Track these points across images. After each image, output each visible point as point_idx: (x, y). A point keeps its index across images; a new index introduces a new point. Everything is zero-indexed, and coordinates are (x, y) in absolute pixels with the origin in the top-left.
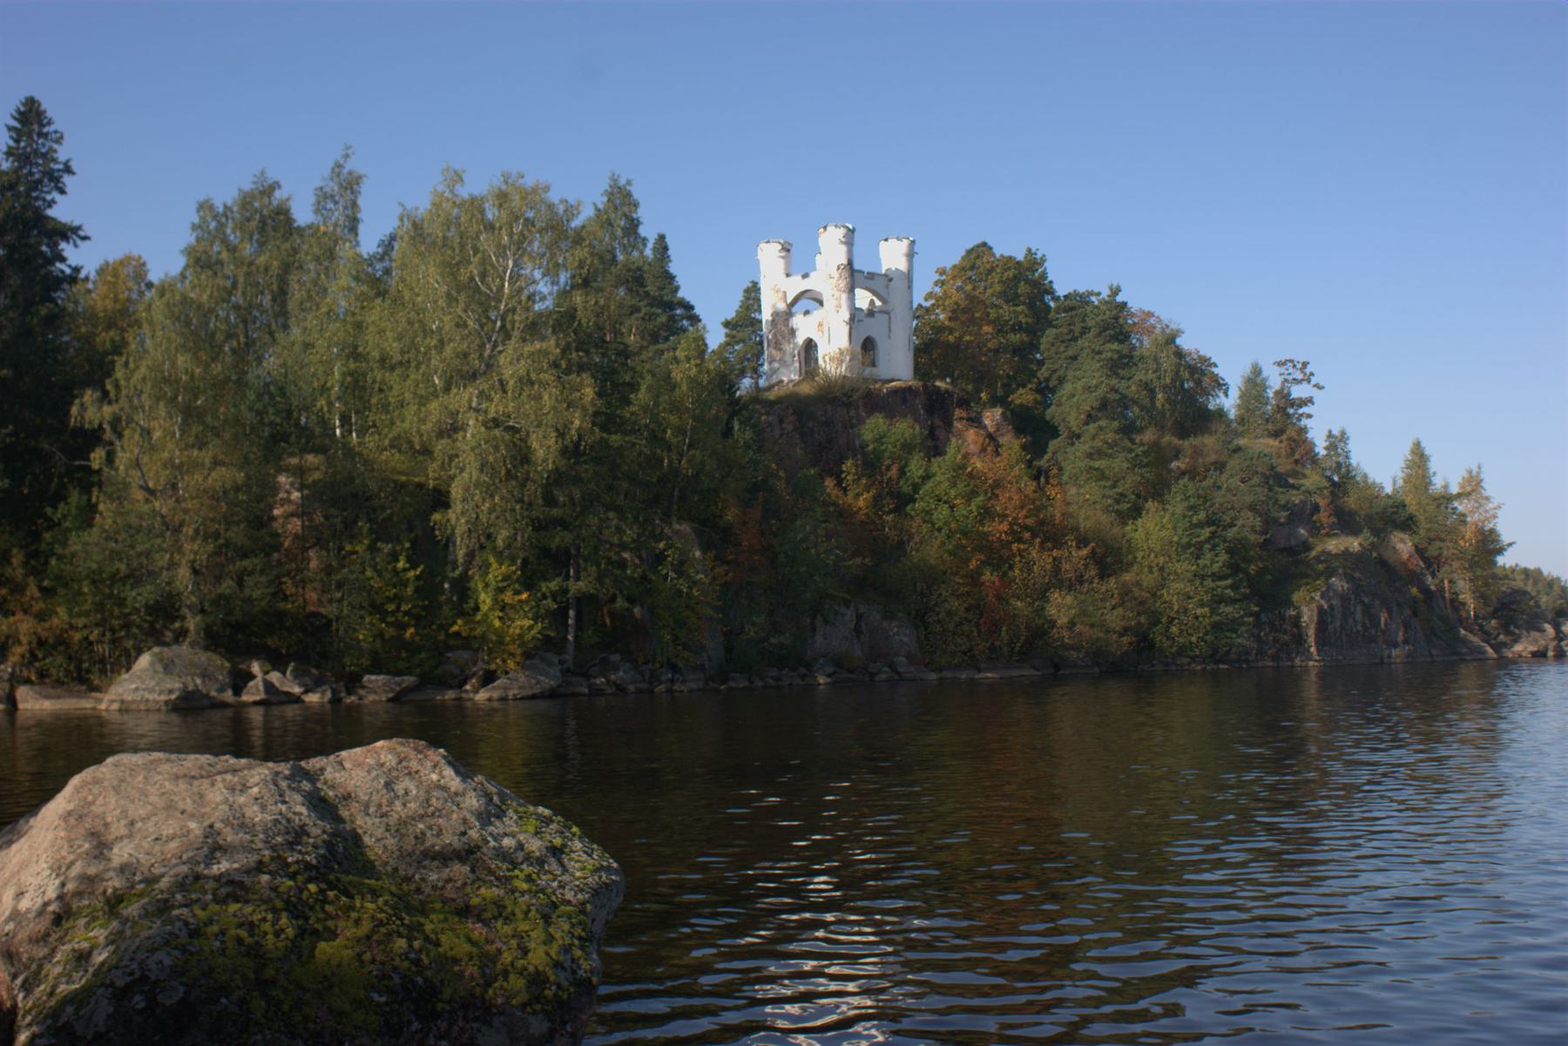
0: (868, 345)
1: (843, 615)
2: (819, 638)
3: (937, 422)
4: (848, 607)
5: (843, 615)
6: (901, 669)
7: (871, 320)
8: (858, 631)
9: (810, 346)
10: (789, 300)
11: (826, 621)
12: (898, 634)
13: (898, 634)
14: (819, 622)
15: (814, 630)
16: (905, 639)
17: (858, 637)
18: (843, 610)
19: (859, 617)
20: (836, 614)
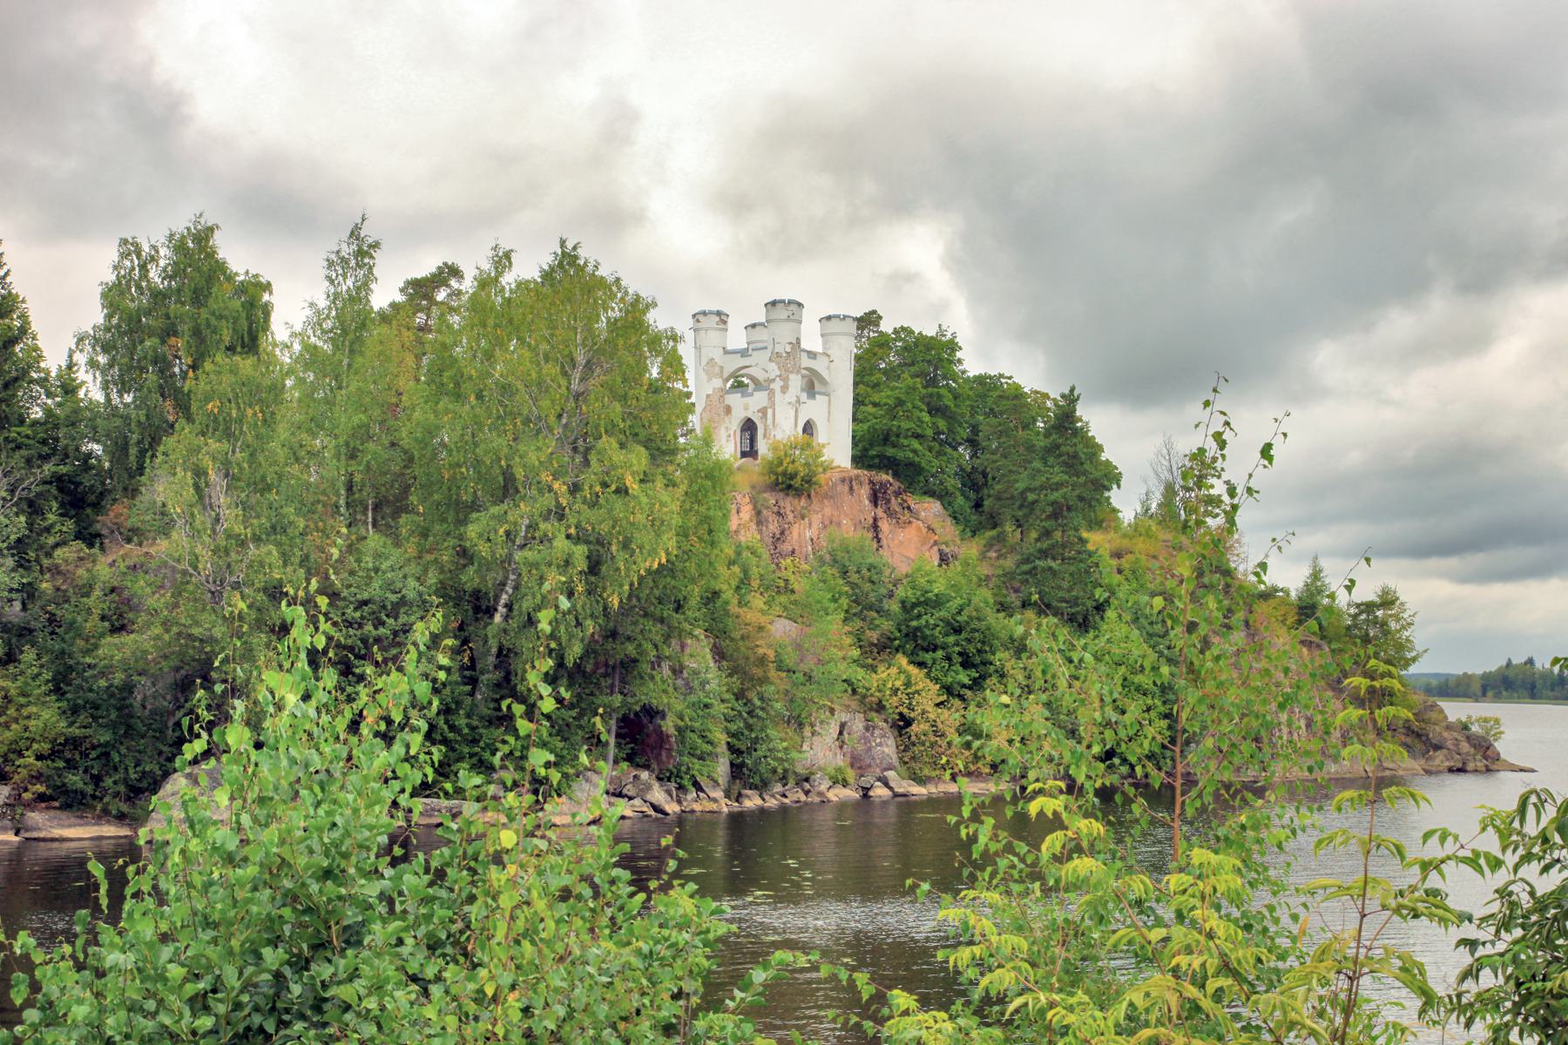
0: (808, 428)
3: (880, 512)
9: (749, 427)
10: (725, 376)
13: (880, 744)
16: (886, 750)
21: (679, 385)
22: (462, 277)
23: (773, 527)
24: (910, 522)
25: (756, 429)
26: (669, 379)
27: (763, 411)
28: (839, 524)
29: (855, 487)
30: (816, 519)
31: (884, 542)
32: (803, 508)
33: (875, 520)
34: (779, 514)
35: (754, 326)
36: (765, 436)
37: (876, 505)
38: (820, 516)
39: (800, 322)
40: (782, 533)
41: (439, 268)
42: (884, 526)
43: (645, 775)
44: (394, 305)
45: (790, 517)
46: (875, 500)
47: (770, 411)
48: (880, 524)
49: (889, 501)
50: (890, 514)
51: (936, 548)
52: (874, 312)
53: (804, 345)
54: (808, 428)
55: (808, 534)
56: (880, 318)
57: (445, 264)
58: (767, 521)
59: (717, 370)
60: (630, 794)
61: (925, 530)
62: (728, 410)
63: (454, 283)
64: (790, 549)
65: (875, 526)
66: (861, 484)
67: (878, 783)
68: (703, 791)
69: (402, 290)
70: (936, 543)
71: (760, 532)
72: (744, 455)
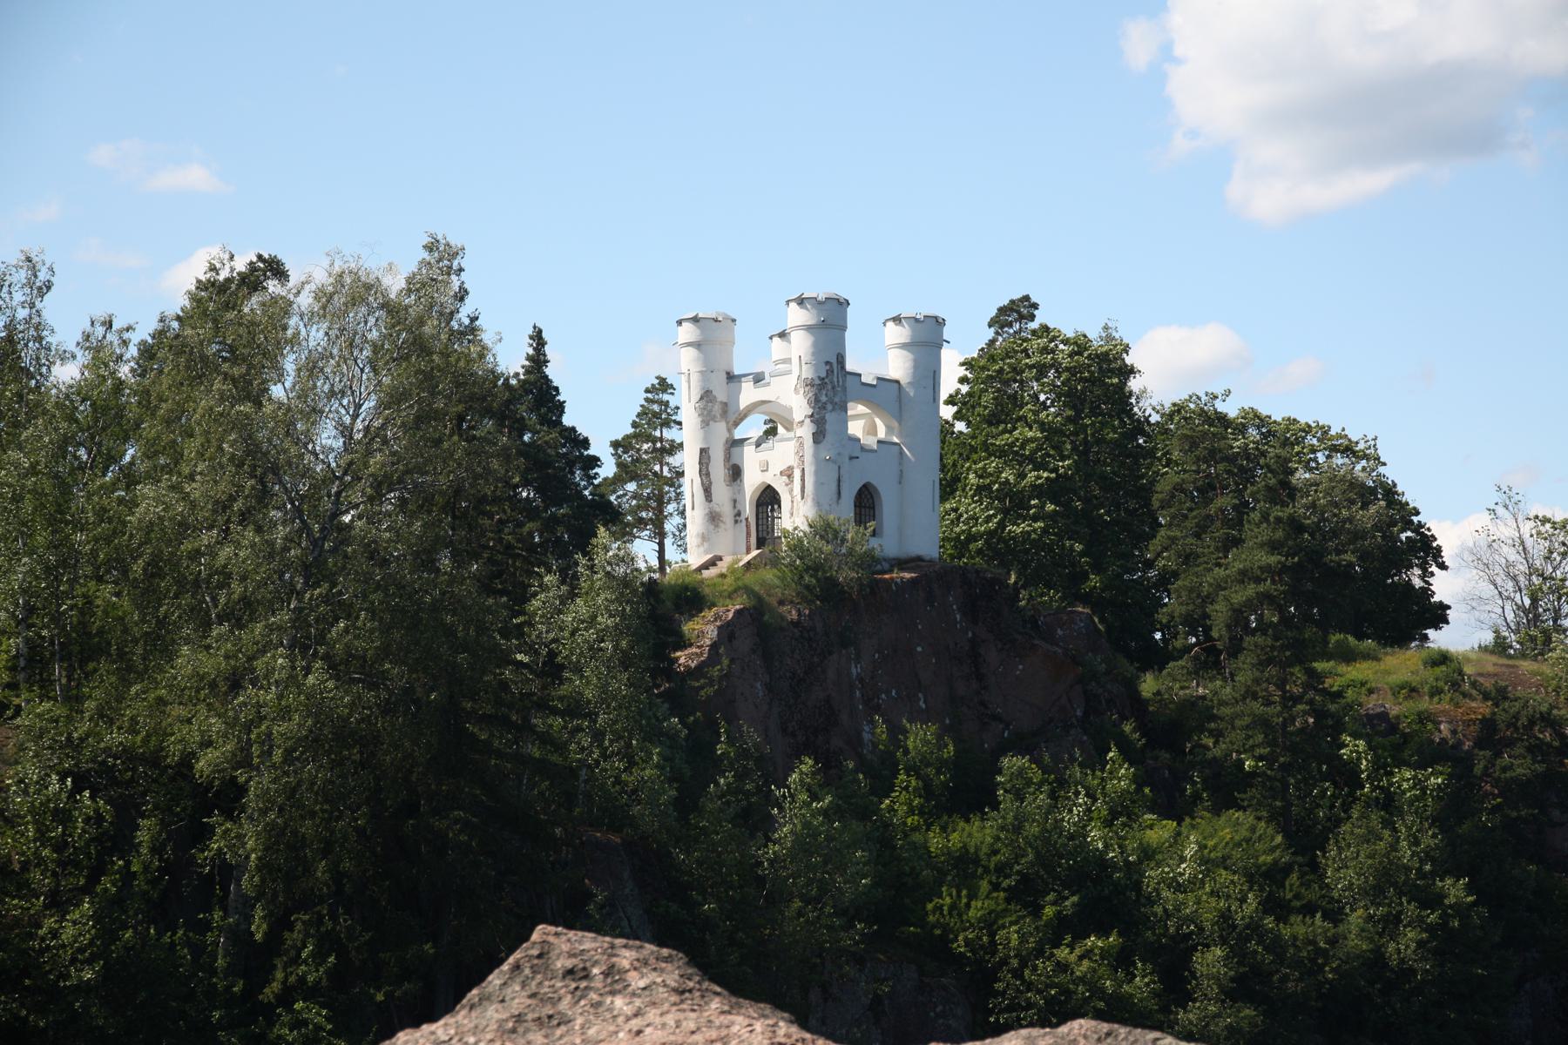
0: (866, 502)
9: (768, 499)
10: (732, 418)
21: (669, 434)
27: (788, 473)
39: (843, 328)
41: (251, 263)
47: (797, 474)
52: (1026, 298)
53: (849, 367)
54: (866, 502)
56: (1035, 306)
57: (260, 257)
59: (717, 409)
62: (736, 473)
63: (273, 286)
72: (761, 543)
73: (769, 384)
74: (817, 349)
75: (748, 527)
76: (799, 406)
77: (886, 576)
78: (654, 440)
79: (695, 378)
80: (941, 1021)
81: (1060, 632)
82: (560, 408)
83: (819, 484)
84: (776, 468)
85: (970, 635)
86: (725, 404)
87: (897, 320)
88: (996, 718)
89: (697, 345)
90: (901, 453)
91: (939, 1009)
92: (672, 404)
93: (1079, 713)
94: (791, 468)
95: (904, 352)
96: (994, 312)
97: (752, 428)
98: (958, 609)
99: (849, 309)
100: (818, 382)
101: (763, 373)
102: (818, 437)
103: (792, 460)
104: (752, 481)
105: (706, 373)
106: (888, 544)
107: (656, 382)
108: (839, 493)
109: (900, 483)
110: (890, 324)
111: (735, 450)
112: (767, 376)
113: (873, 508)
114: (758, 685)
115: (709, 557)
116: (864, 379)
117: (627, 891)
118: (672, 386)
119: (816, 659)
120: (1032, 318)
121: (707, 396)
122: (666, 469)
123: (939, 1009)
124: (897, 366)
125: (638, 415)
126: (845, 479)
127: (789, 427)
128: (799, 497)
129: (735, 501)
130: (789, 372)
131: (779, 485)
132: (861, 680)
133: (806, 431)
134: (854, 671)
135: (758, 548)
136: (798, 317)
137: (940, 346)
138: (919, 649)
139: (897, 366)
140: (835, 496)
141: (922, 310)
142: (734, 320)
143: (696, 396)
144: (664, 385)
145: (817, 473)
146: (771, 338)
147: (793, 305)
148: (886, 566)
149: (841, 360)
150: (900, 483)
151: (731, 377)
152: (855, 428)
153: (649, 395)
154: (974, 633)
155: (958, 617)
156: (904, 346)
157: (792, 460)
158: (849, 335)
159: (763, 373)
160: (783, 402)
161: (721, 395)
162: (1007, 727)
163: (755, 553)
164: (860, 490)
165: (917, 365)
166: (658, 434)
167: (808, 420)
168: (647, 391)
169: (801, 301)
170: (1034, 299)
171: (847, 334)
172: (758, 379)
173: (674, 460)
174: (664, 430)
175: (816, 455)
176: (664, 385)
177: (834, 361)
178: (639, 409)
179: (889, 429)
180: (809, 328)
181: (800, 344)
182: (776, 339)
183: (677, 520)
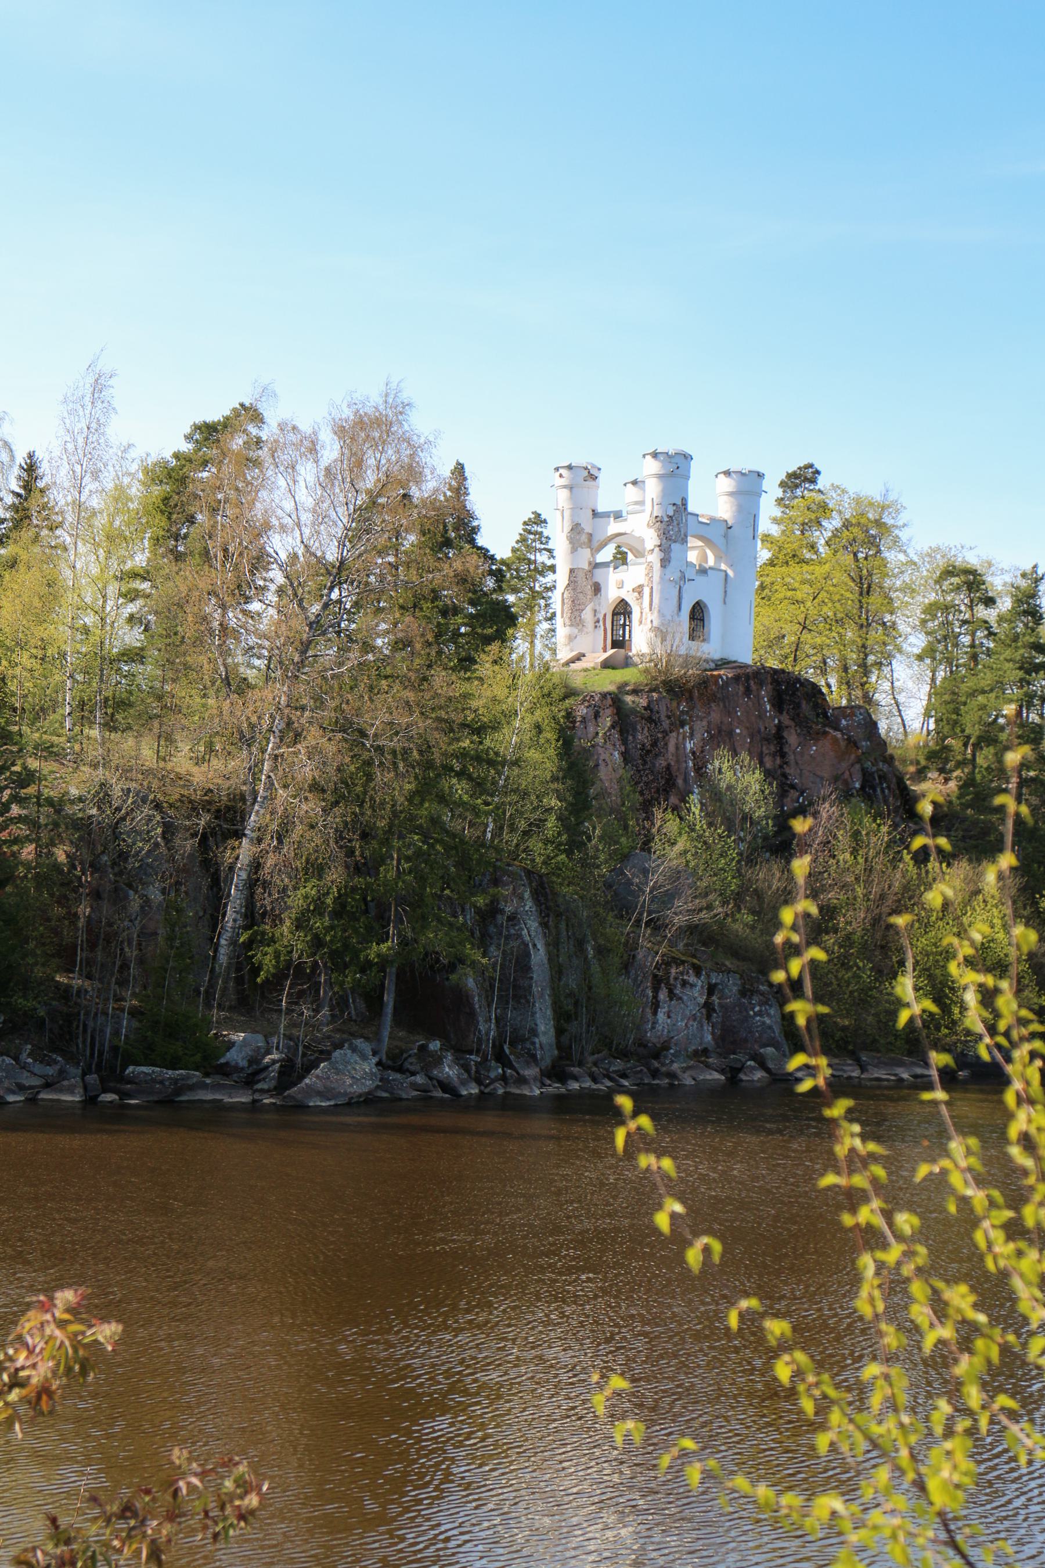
0: (698, 614)
1: (692, 986)
2: (661, 1016)
4: (698, 974)
5: (692, 986)
6: (771, 1065)
7: (701, 579)
8: (708, 1006)
9: (622, 610)
11: (672, 995)
12: (760, 1014)
13: (760, 1014)
14: (663, 995)
15: (656, 1006)
16: (768, 1021)
17: (709, 1017)
18: (692, 979)
19: (711, 989)
20: (684, 983)
21: (542, 558)
22: (262, 421)
23: (642, 736)
24: (825, 733)
25: (630, 613)
26: (530, 549)
27: (639, 590)
28: (731, 733)
29: (753, 687)
30: (700, 726)
31: (791, 758)
32: (682, 712)
33: (780, 728)
34: (650, 720)
35: (635, 483)
36: (641, 622)
37: (781, 711)
38: (705, 723)
39: (688, 478)
40: (654, 744)
41: (234, 410)
42: (792, 738)
43: (435, 1045)
44: (177, 456)
45: (666, 724)
46: (778, 704)
47: (646, 591)
48: (785, 734)
49: (798, 706)
50: (799, 720)
51: (858, 766)
52: (811, 466)
53: (691, 508)
54: (698, 614)
55: (689, 746)
56: (818, 472)
57: (242, 405)
58: (635, 729)
59: (584, 538)
60: (412, 1068)
61: (843, 744)
62: (597, 589)
64: (664, 764)
65: (778, 737)
66: (761, 684)
67: (751, 1063)
68: (512, 1067)
69: (188, 438)
70: (859, 760)
71: (624, 742)
73: (626, 520)
74: (665, 493)
75: (605, 630)
76: (651, 538)
77: (715, 673)
78: (530, 562)
79: (567, 514)
80: (758, 1018)
81: (844, 722)
82: (475, 530)
83: (664, 599)
84: (629, 585)
85: (776, 721)
86: (591, 535)
87: (727, 473)
88: (793, 787)
89: (570, 488)
90: (726, 575)
91: (757, 1009)
92: (545, 534)
93: (857, 785)
94: (641, 586)
95: (732, 499)
96: (783, 476)
97: (606, 555)
98: (769, 701)
99: (692, 463)
100: (666, 519)
101: (621, 511)
102: (665, 562)
103: (642, 580)
104: (612, 593)
105: (576, 507)
106: (712, 649)
107: (533, 516)
108: (680, 609)
109: (725, 603)
110: (722, 476)
111: (598, 572)
112: (624, 514)
113: (702, 620)
114: (616, 753)
115: (574, 653)
116: (700, 519)
117: (527, 908)
118: (545, 522)
119: (660, 735)
120: (813, 481)
121: (576, 529)
122: (537, 585)
123: (757, 1009)
124: (724, 509)
125: (517, 542)
126: (685, 595)
127: (639, 554)
128: (648, 609)
129: (595, 611)
130: (643, 511)
131: (631, 599)
132: (694, 753)
133: (655, 558)
134: (689, 746)
135: (612, 648)
136: (652, 467)
137: (760, 496)
138: (738, 731)
139: (724, 509)
140: (676, 609)
141: (747, 466)
142: (599, 469)
143: (567, 527)
144: (538, 520)
145: (662, 592)
146: (625, 485)
147: (648, 457)
148: (713, 665)
149: (684, 503)
150: (725, 603)
151: (595, 514)
152: (693, 557)
153: (529, 527)
154: (779, 721)
155: (768, 707)
156: (731, 494)
157: (642, 580)
158: (691, 483)
159: (621, 511)
160: (637, 534)
161: (587, 526)
162: (802, 794)
163: (611, 652)
164: (694, 607)
165: (740, 509)
166: (533, 558)
167: (657, 549)
168: (525, 523)
169: (655, 455)
170: (818, 466)
171: (690, 482)
172: (618, 516)
173: (548, 579)
174: (538, 554)
175: (661, 578)
176: (538, 520)
177: (679, 503)
178: (518, 538)
179: (718, 558)
180: (660, 477)
181: (653, 489)
182: (630, 486)
183: (545, 625)
